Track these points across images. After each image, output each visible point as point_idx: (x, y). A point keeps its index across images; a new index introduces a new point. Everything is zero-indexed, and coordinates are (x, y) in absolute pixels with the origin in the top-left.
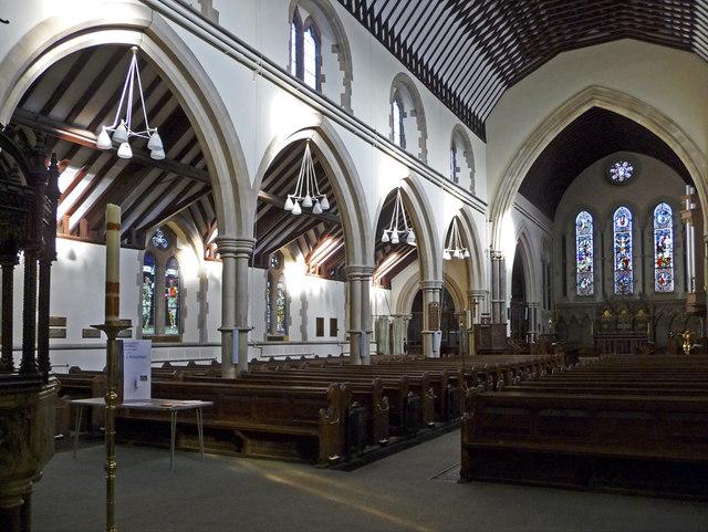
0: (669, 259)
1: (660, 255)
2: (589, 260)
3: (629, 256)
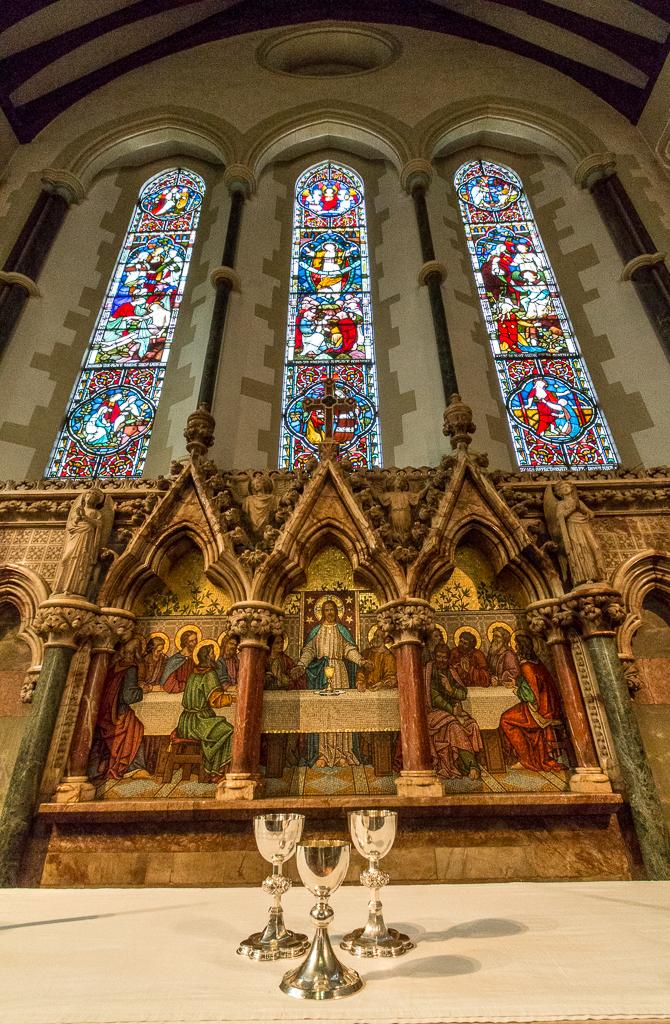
0: (549, 322)
1: (507, 306)
2: (161, 315)
3: (357, 306)
